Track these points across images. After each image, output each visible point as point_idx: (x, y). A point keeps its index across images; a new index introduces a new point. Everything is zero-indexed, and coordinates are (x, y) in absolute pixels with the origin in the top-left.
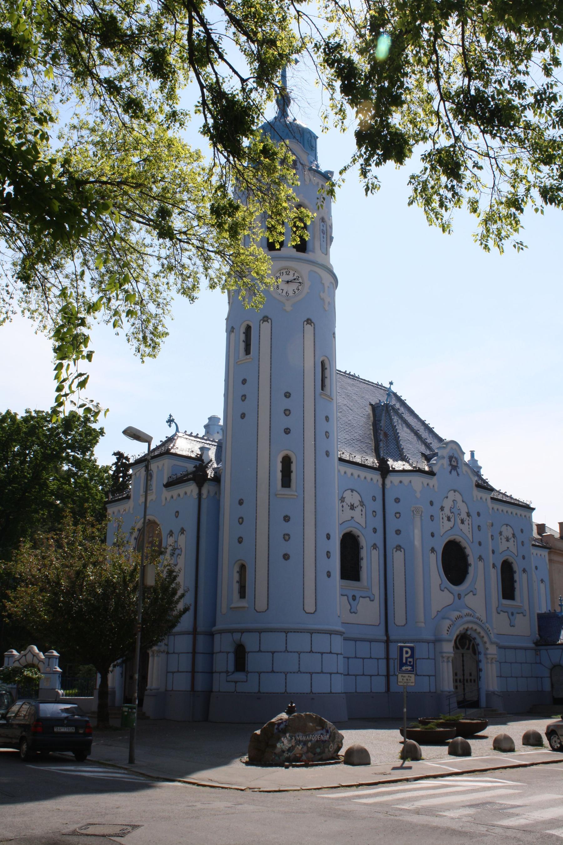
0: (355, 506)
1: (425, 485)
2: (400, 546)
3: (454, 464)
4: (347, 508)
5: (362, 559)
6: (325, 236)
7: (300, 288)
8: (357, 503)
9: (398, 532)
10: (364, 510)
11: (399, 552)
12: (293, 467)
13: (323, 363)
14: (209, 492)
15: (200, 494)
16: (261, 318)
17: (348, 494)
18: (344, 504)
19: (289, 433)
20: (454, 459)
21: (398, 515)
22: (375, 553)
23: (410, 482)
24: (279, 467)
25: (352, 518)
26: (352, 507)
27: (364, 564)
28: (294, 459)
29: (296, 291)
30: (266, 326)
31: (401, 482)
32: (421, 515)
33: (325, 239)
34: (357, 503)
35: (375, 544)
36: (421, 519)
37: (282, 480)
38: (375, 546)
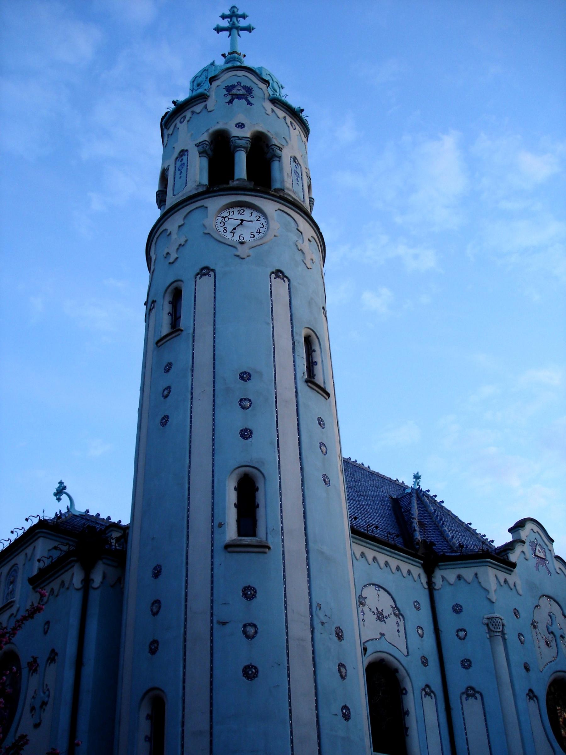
0: (385, 614)
1: (502, 582)
2: (472, 688)
3: (542, 555)
4: (370, 618)
5: (407, 713)
6: (300, 179)
7: (262, 230)
8: (388, 611)
9: (466, 664)
10: (401, 623)
11: (471, 700)
12: (260, 497)
13: (308, 340)
14: (104, 577)
15: (87, 582)
17: (370, 593)
18: (366, 609)
19: (250, 436)
20: (538, 548)
21: (462, 634)
22: (429, 703)
23: (476, 574)
24: (232, 497)
25: (383, 635)
26: (380, 617)
27: (412, 722)
28: (260, 485)
29: (256, 235)
30: (206, 283)
31: (459, 577)
32: (503, 633)
33: (300, 183)
34: (388, 611)
35: (427, 686)
36: (504, 640)
37: (239, 521)
38: (427, 690)
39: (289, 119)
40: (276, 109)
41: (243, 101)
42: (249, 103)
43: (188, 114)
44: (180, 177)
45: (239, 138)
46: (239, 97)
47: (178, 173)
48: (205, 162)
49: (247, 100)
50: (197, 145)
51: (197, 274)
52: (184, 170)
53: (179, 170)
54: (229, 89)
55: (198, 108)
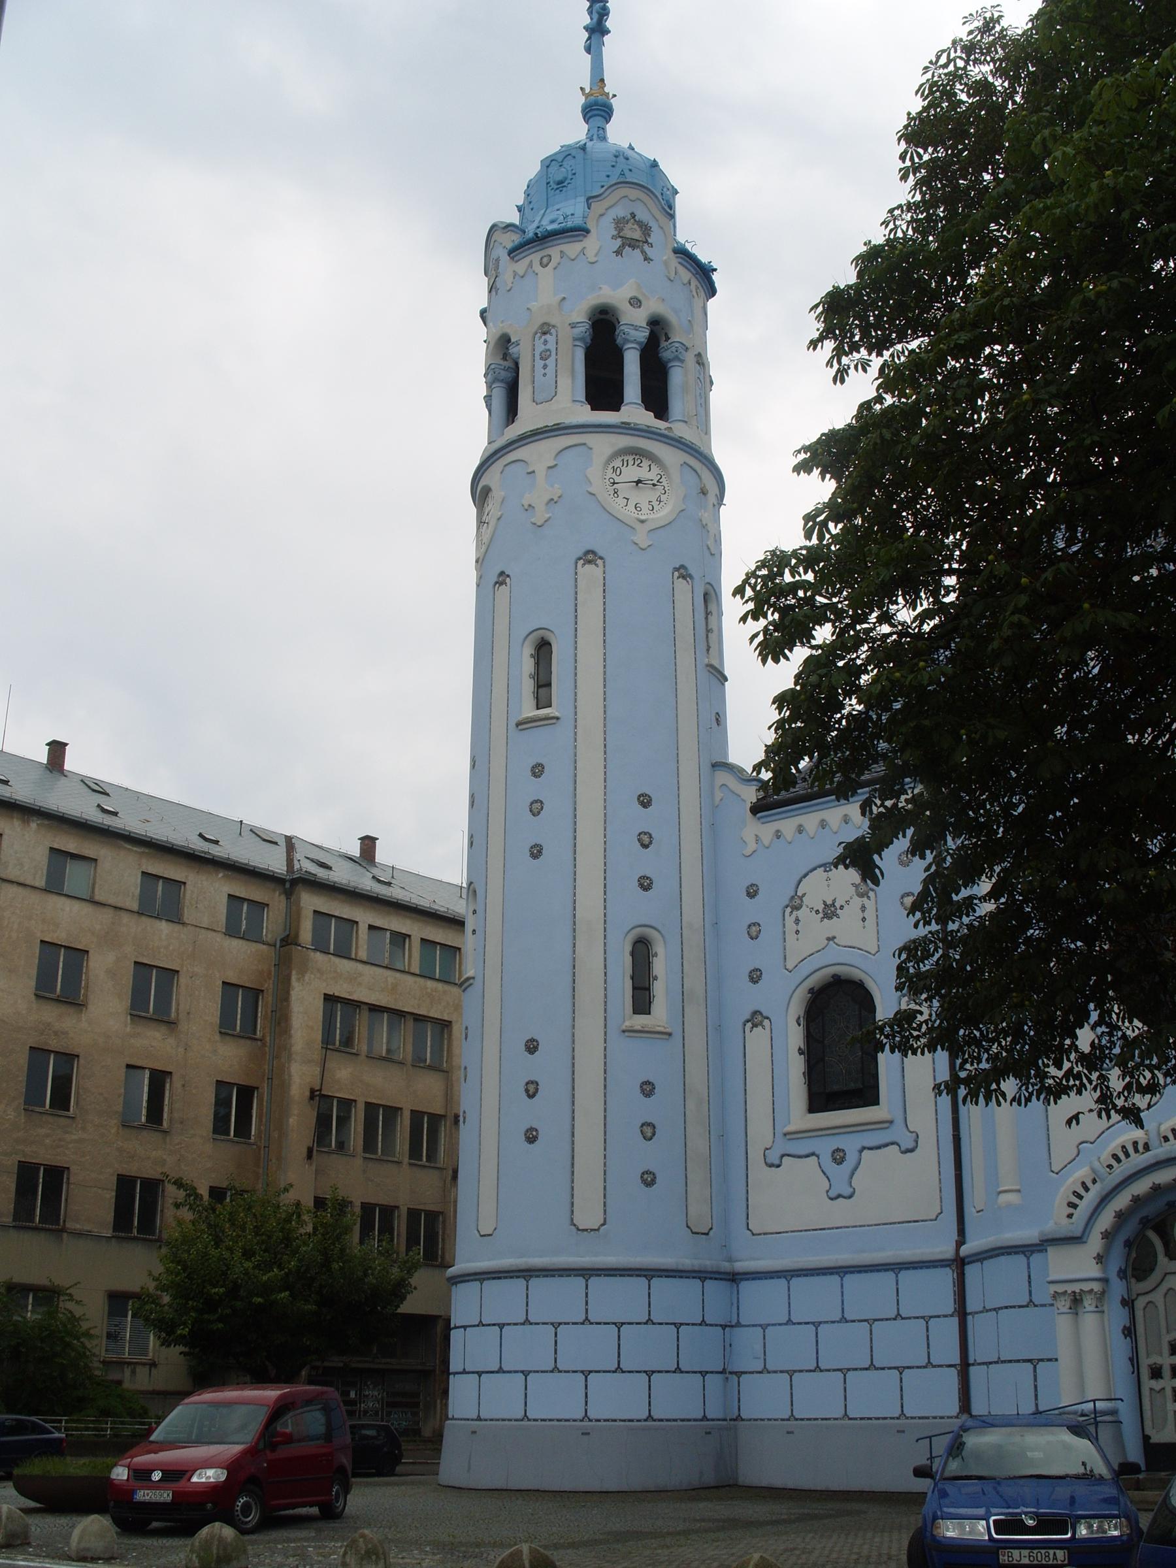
7: (663, 498)
16: (580, 553)
29: (655, 503)
39: (694, 282)
40: (681, 270)
41: (637, 252)
42: (647, 259)
43: (554, 252)
44: (545, 375)
45: (636, 328)
46: (633, 244)
47: (539, 363)
48: (580, 355)
49: (643, 252)
50: (573, 326)
51: (580, 559)
52: (551, 362)
53: (541, 358)
54: (620, 223)
55: (572, 248)
